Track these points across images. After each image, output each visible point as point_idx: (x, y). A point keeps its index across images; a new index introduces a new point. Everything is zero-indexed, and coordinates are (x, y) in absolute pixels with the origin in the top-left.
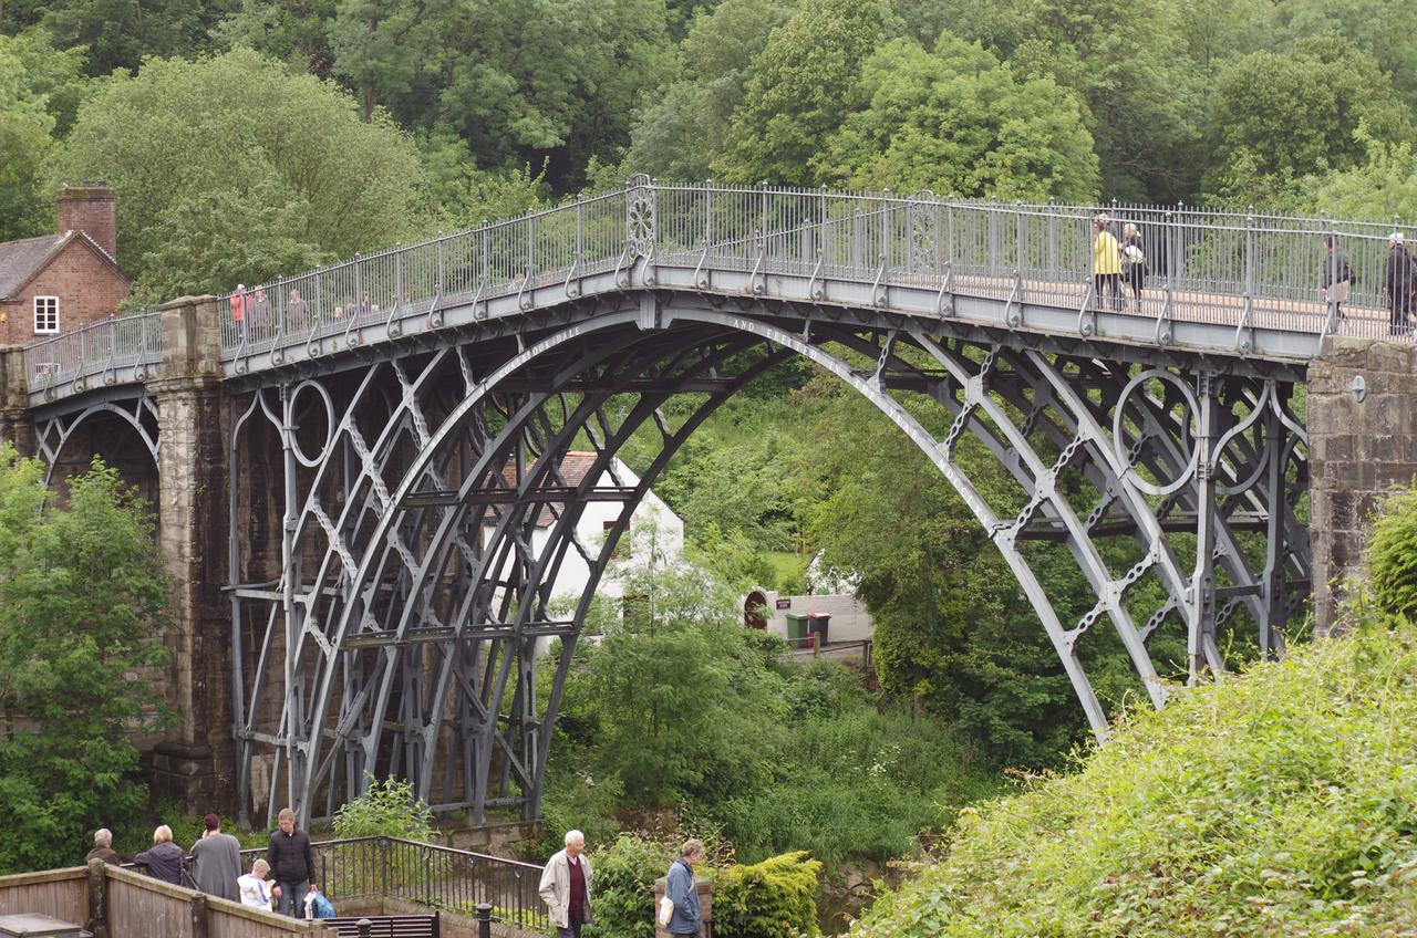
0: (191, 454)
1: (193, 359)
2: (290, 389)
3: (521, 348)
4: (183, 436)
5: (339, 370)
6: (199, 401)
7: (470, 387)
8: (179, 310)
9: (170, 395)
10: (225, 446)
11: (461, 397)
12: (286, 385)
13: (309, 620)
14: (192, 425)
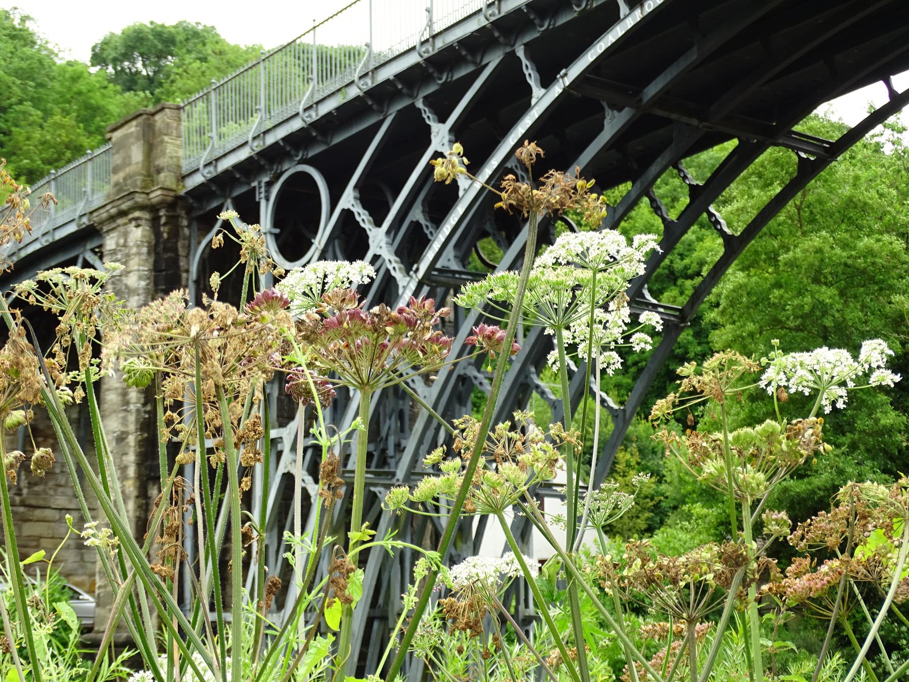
0: (143, 283)
1: (151, 172)
2: (269, 184)
3: (624, 9)
4: (134, 263)
5: (337, 140)
6: (155, 222)
7: (537, 91)
8: (134, 123)
9: (120, 221)
10: (184, 275)
11: (526, 107)
12: (266, 179)
13: (286, 456)
14: (145, 250)
